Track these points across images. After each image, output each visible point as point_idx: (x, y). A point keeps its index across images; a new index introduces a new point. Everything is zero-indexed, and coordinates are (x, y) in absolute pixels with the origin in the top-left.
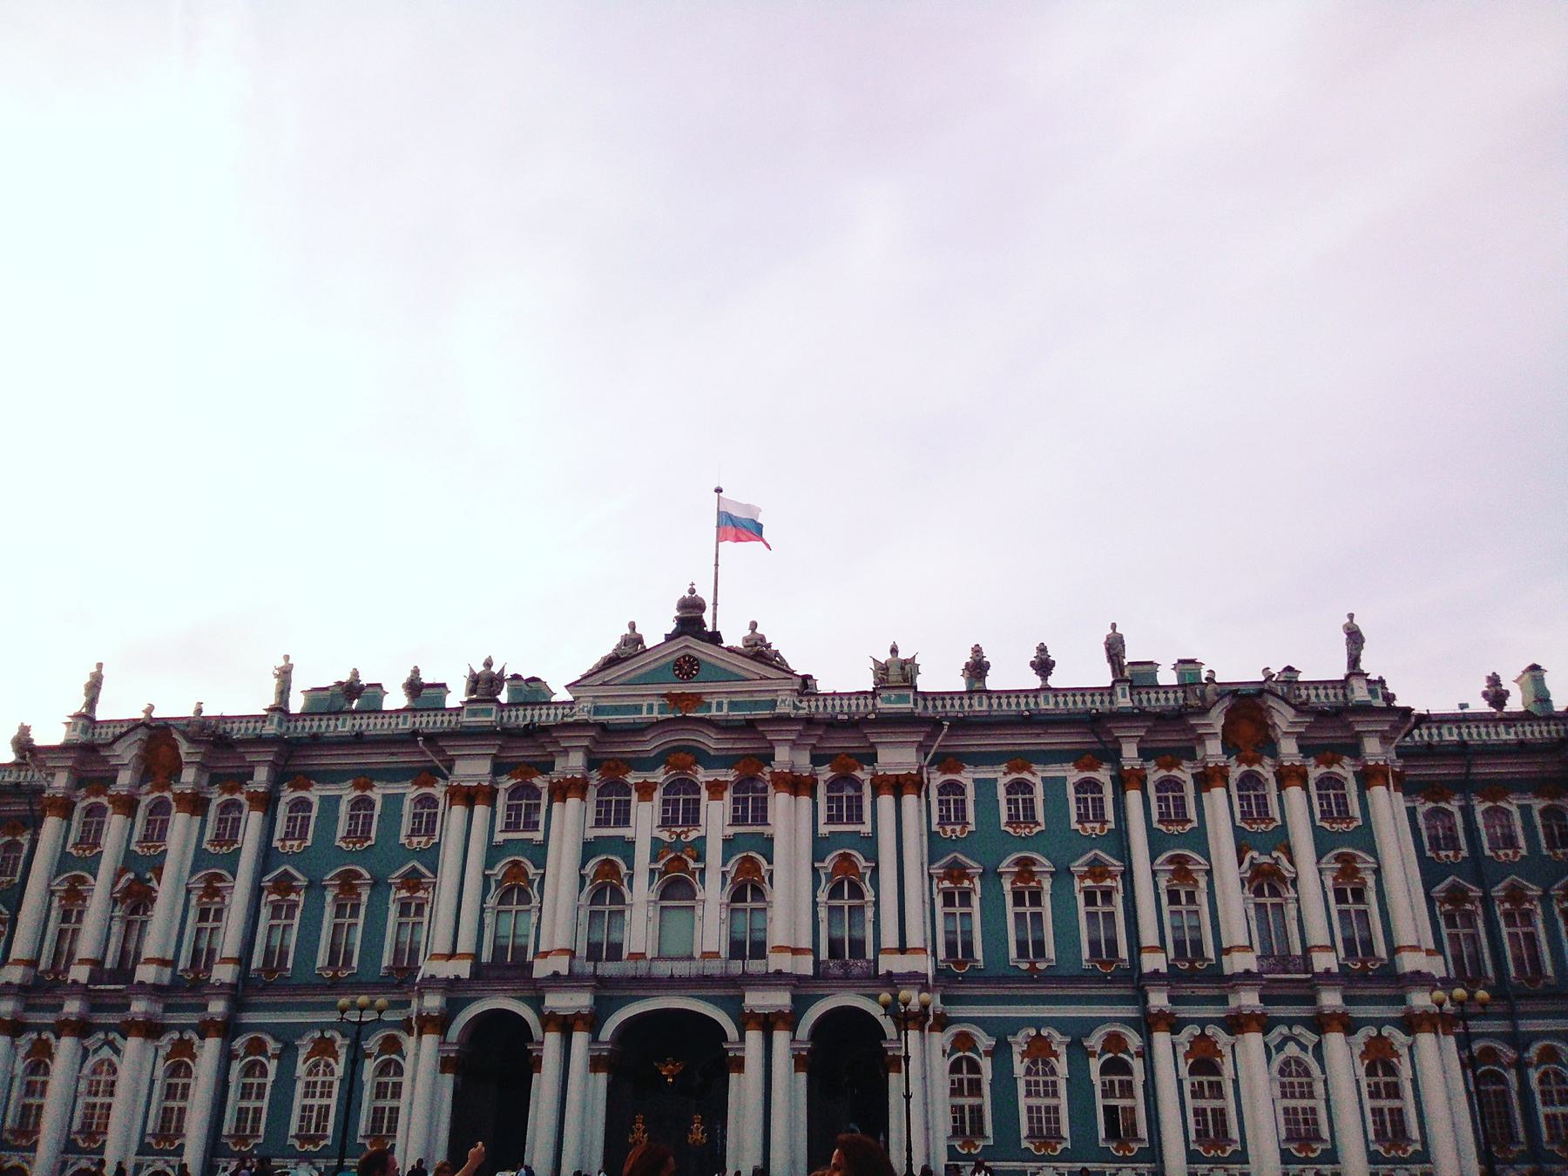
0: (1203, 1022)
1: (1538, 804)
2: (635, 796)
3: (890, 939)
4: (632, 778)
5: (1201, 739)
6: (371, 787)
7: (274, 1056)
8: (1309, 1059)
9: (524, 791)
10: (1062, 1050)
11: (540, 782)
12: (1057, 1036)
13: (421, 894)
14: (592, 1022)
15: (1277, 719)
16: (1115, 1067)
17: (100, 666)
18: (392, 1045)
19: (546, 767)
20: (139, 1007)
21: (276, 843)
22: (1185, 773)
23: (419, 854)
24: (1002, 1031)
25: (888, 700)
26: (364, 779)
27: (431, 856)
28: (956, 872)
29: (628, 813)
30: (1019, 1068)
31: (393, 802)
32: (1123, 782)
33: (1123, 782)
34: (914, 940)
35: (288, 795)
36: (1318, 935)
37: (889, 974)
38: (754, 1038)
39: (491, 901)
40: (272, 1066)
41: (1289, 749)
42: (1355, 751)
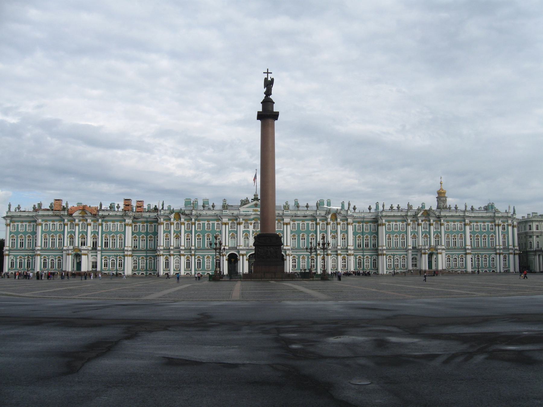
1: (372, 224)
3: (285, 244)
4: (249, 222)
11: (235, 222)
14: (246, 255)
19: (237, 220)
20: (182, 252)
22: (325, 223)
26: (208, 220)
27: (221, 232)
30: (301, 260)
31: (213, 224)
32: (317, 224)
33: (317, 224)
34: (289, 244)
35: (197, 223)
36: (339, 244)
41: (339, 220)
42: (347, 220)
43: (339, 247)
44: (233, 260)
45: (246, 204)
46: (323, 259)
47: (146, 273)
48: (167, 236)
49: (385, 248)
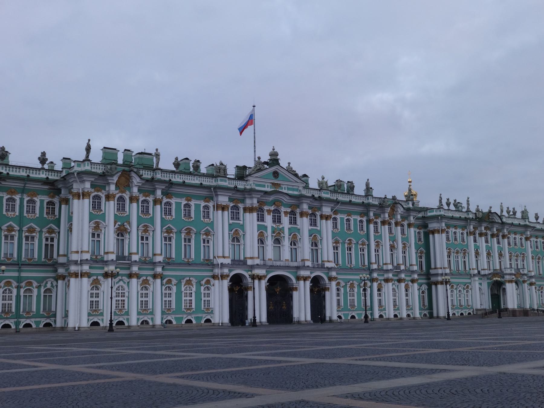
0: (381, 280)
2: (266, 213)
3: (325, 259)
4: (266, 208)
5: (384, 213)
6: (190, 200)
7: (175, 285)
8: (396, 288)
9: (236, 207)
10: (356, 286)
11: (241, 206)
12: (356, 283)
13: (209, 237)
14: (265, 277)
15: (399, 210)
16: (365, 290)
17: (89, 140)
18: (208, 282)
19: (243, 201)
21: (164, 216)
22: (379, 221)
23: (208, 224)
24: (347, 281)
25: (324, 193)
26: (189, 198)
28: (337, 242)
29: (263, 218)
30: (348, 290)
32: (369, 221)
33: (369, 221)
35: (165, 200)
37: (327, 267)
38: (302, 282)
39: (231, 242)
40: (174, 288)
43: (402, 267)
44: (237, 289)
45: (260, 170)
46: (379, 290)
47: (17, 324)
48: (97, 227)
49: (448, 271)
